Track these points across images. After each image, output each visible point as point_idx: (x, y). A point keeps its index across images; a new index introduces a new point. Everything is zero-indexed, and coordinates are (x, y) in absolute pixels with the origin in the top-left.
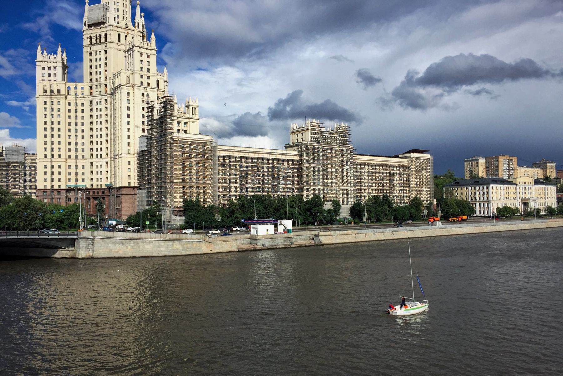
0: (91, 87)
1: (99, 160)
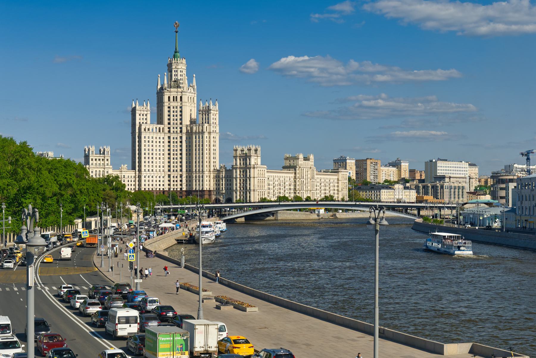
0: (169, 128)
1: (175, 173)
